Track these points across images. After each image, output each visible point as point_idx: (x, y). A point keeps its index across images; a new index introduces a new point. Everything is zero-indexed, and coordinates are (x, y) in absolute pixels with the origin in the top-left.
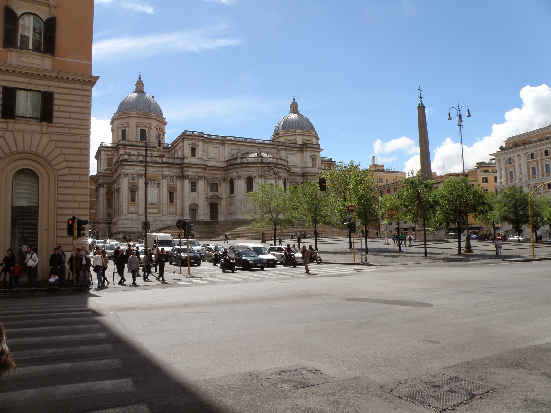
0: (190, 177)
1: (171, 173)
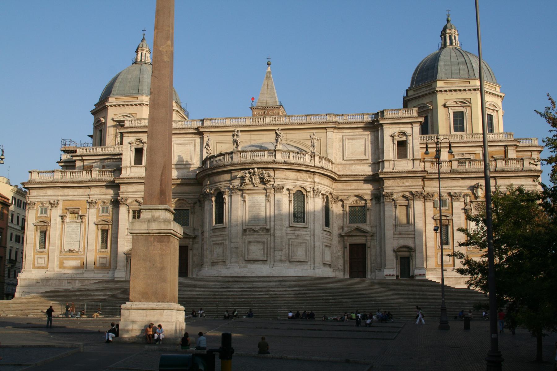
0: (129, 201)
1: (103, 197)
